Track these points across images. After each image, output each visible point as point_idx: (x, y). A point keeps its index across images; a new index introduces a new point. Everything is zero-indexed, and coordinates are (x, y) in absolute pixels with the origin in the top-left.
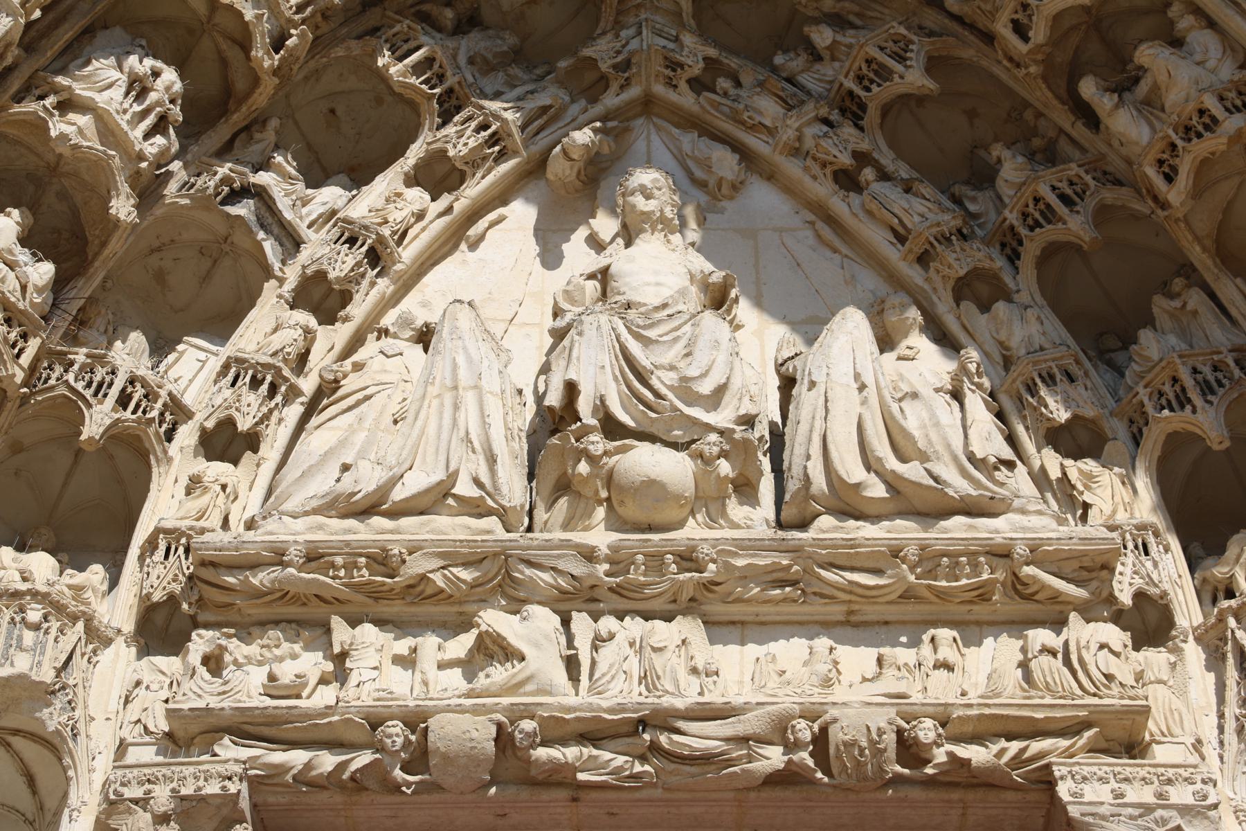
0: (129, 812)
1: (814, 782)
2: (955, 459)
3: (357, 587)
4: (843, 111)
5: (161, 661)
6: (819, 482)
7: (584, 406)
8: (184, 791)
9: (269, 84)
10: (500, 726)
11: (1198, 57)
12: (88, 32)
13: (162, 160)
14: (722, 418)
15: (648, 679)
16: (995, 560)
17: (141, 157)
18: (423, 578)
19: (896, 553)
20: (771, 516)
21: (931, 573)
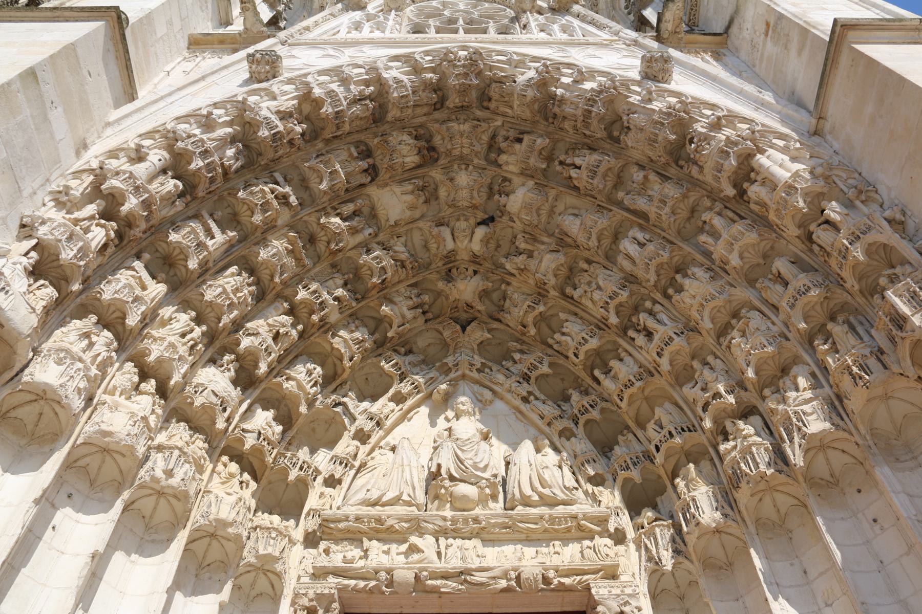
0: (301, 598)
1: (516, 591)
2: (560, 487)
3: (371, 529)
4: (524, 379)
5: (311, 550)
6: (518, 495)
7: (443, 471)
8: (318, 592)
9: (348, 371)
10: (416, 574)
12: (296, 357)
13: (315, 394)
14: (487, 475)
15: (463, 559)
16: (573, 519)
17: (309, 394)
18: (392, 526)
19: (542, 517)
20: (503, 506)
21: (553, 524)
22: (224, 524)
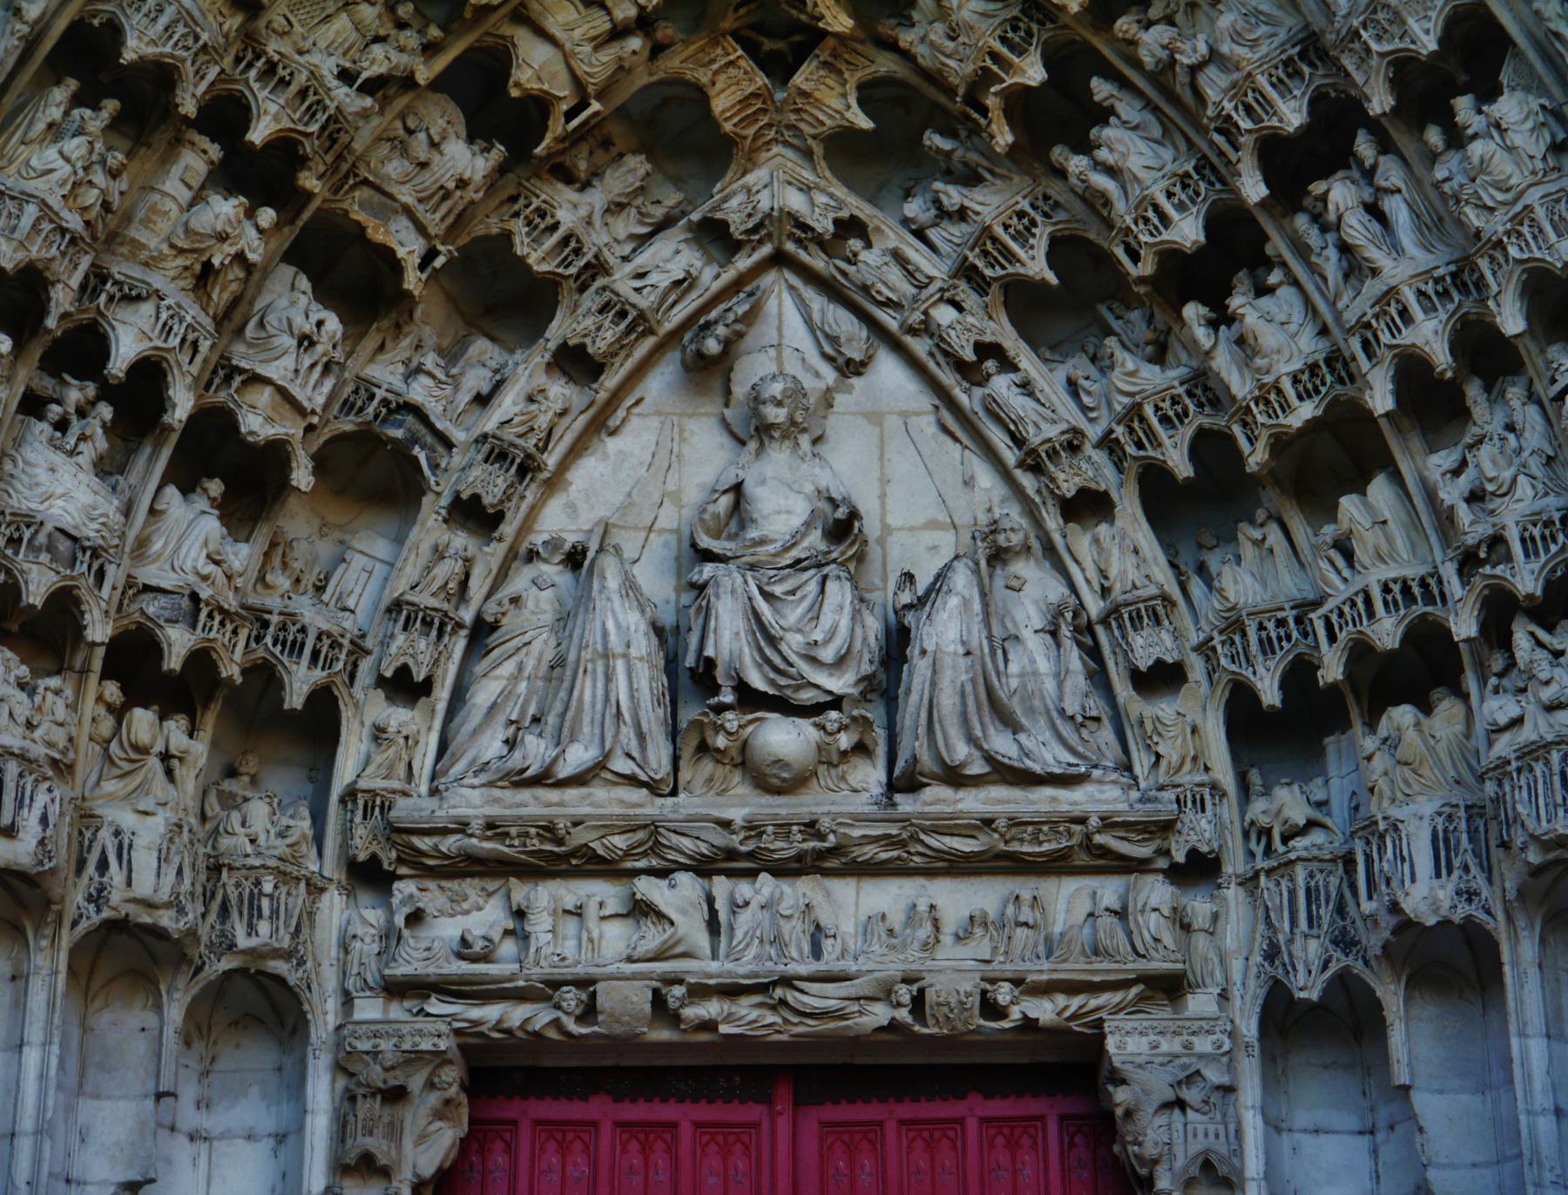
2: (1048, 711)
10: (656, 992)
11: (1282, 317)
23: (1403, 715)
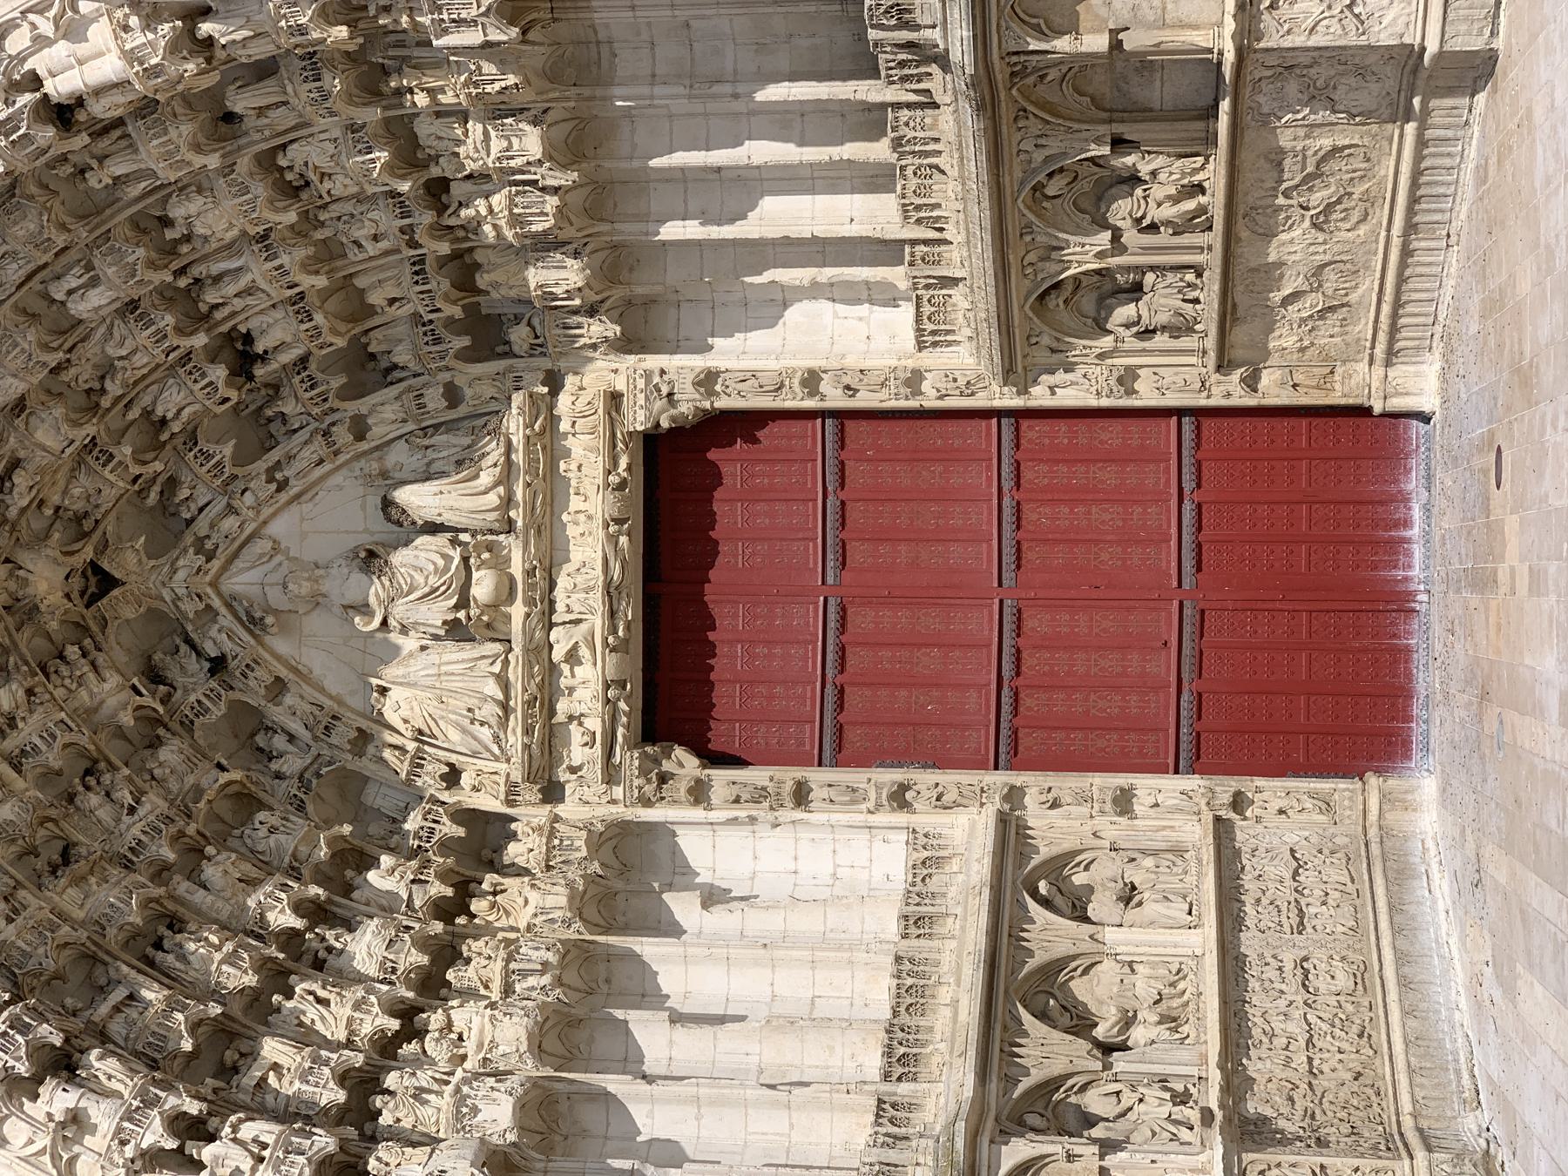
22: (571, 898)
23: (482, 280)
